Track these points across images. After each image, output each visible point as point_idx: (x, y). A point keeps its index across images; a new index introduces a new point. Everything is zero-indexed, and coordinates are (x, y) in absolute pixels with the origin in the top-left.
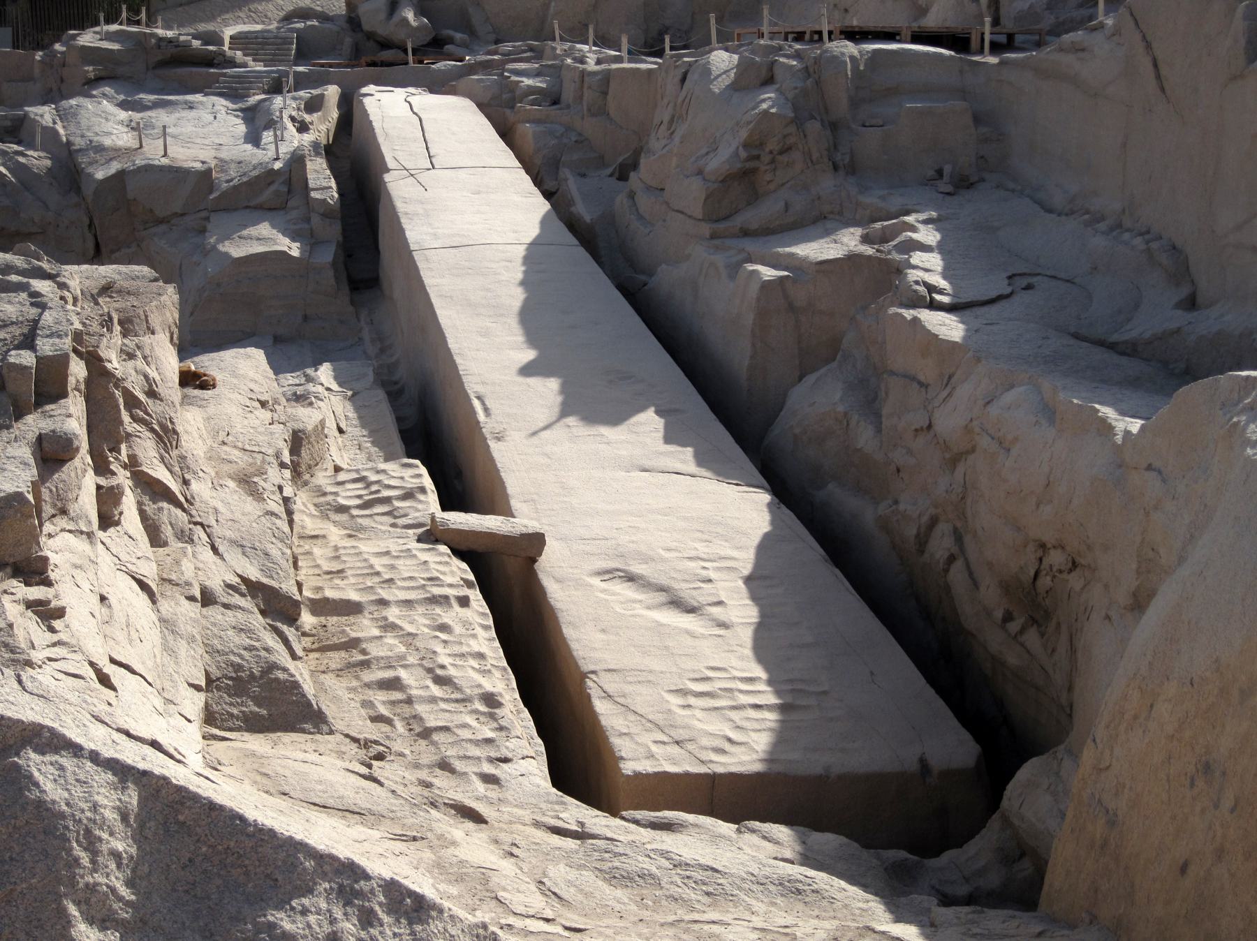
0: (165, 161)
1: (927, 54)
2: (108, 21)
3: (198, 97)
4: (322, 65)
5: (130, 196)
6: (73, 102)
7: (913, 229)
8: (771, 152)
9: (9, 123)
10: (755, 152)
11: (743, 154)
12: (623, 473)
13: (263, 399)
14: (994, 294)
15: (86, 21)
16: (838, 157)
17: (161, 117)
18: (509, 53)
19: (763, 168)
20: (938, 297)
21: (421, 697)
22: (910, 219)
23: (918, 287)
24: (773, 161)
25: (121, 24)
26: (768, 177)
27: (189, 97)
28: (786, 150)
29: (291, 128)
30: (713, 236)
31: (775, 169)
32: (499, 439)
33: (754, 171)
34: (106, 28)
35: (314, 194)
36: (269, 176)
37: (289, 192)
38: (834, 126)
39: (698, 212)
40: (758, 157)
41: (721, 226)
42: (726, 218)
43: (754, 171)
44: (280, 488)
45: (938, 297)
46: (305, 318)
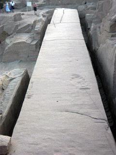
5: (4, 30)
12: (60, 113)
32: (29, 98)
35: (35, 29)
37: (32, 29)
39: (108, 30)
46: (28, 56)
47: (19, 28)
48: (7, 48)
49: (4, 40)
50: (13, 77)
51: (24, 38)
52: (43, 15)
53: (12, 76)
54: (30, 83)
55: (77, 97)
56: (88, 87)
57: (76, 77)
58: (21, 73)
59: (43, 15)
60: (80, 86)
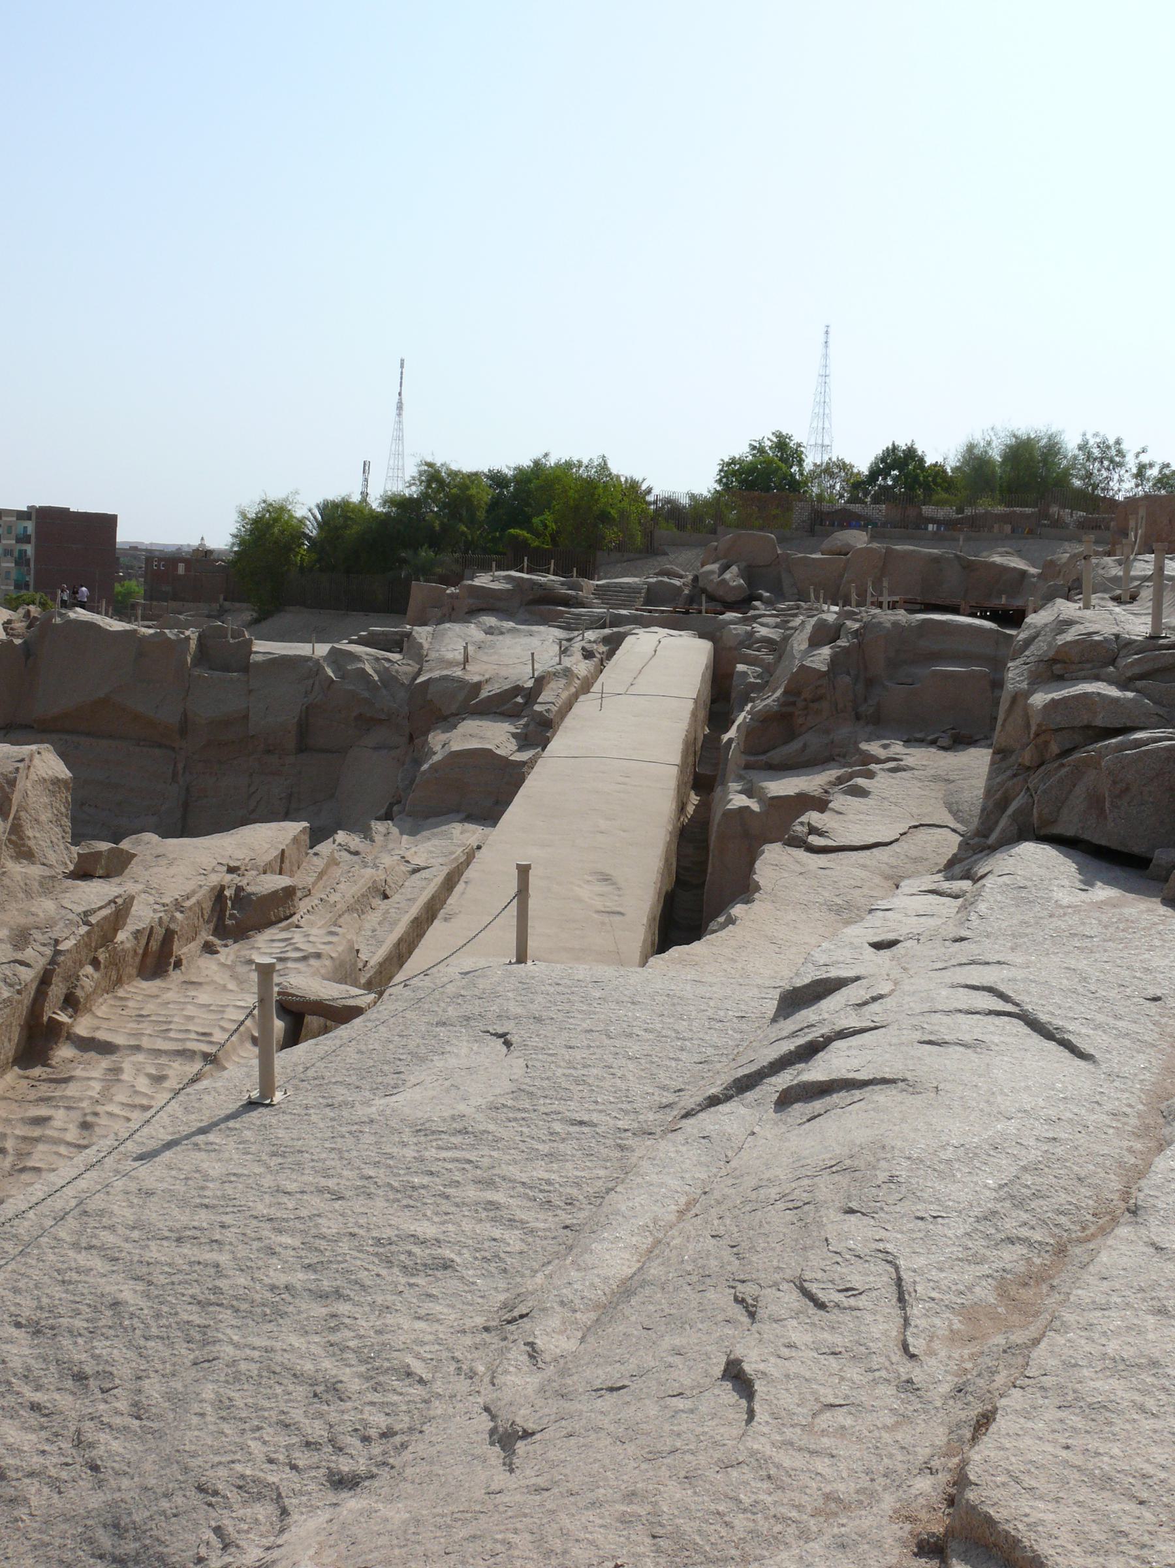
0: (458, 672)
1: (970, 625)
2: (499, 568)
3: (542, 628)
4: (650, 611)
5: (429, 697)
6: (448, 625)
7: (870, 775)
8: (805, 700)
9: (398, 637)
10: (792, 699)
11: (782, 700)
13: (232, 864)
14: (872, 840)
15: (485, 567)
16: (862, 709)
17: (507, 640)
18: (783, 610)
19: (797, 713)
20: (814, 840)
21: (52, 1137)
22: (873, 766)
23: (799, 828)
24: (806, 708)
25: (521, 571)
26: (800, 721)
27: (534, 628)
28: (819, 698)
29: (578, 655)
30: (748, 767)
31: (806, 715)
32: (446, 920)
33: (791, 715)
34: (497, 573)
35: (537, 708)
36: (517, 690)
37: (526, 703)
38: (870, 683)
40: (794, 704)
41: (752, 758)
42: (765, 752)
43: (791, 715)
44: (57, 942)
45: (814, 840)
47: (484, 694)
48: (425, 767)
49: (426, 733)
50: (423, 864)
51: (496, 736)
52: (583, 649)
53: (419, 861)
54: (461, 882)
55: (578, 932)
56: (618, 909)
57: (599, 880)
58: (452, 853)
59: (583, 649)
60: (599, 904)
